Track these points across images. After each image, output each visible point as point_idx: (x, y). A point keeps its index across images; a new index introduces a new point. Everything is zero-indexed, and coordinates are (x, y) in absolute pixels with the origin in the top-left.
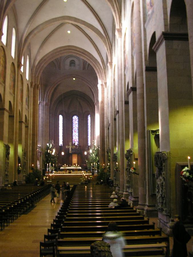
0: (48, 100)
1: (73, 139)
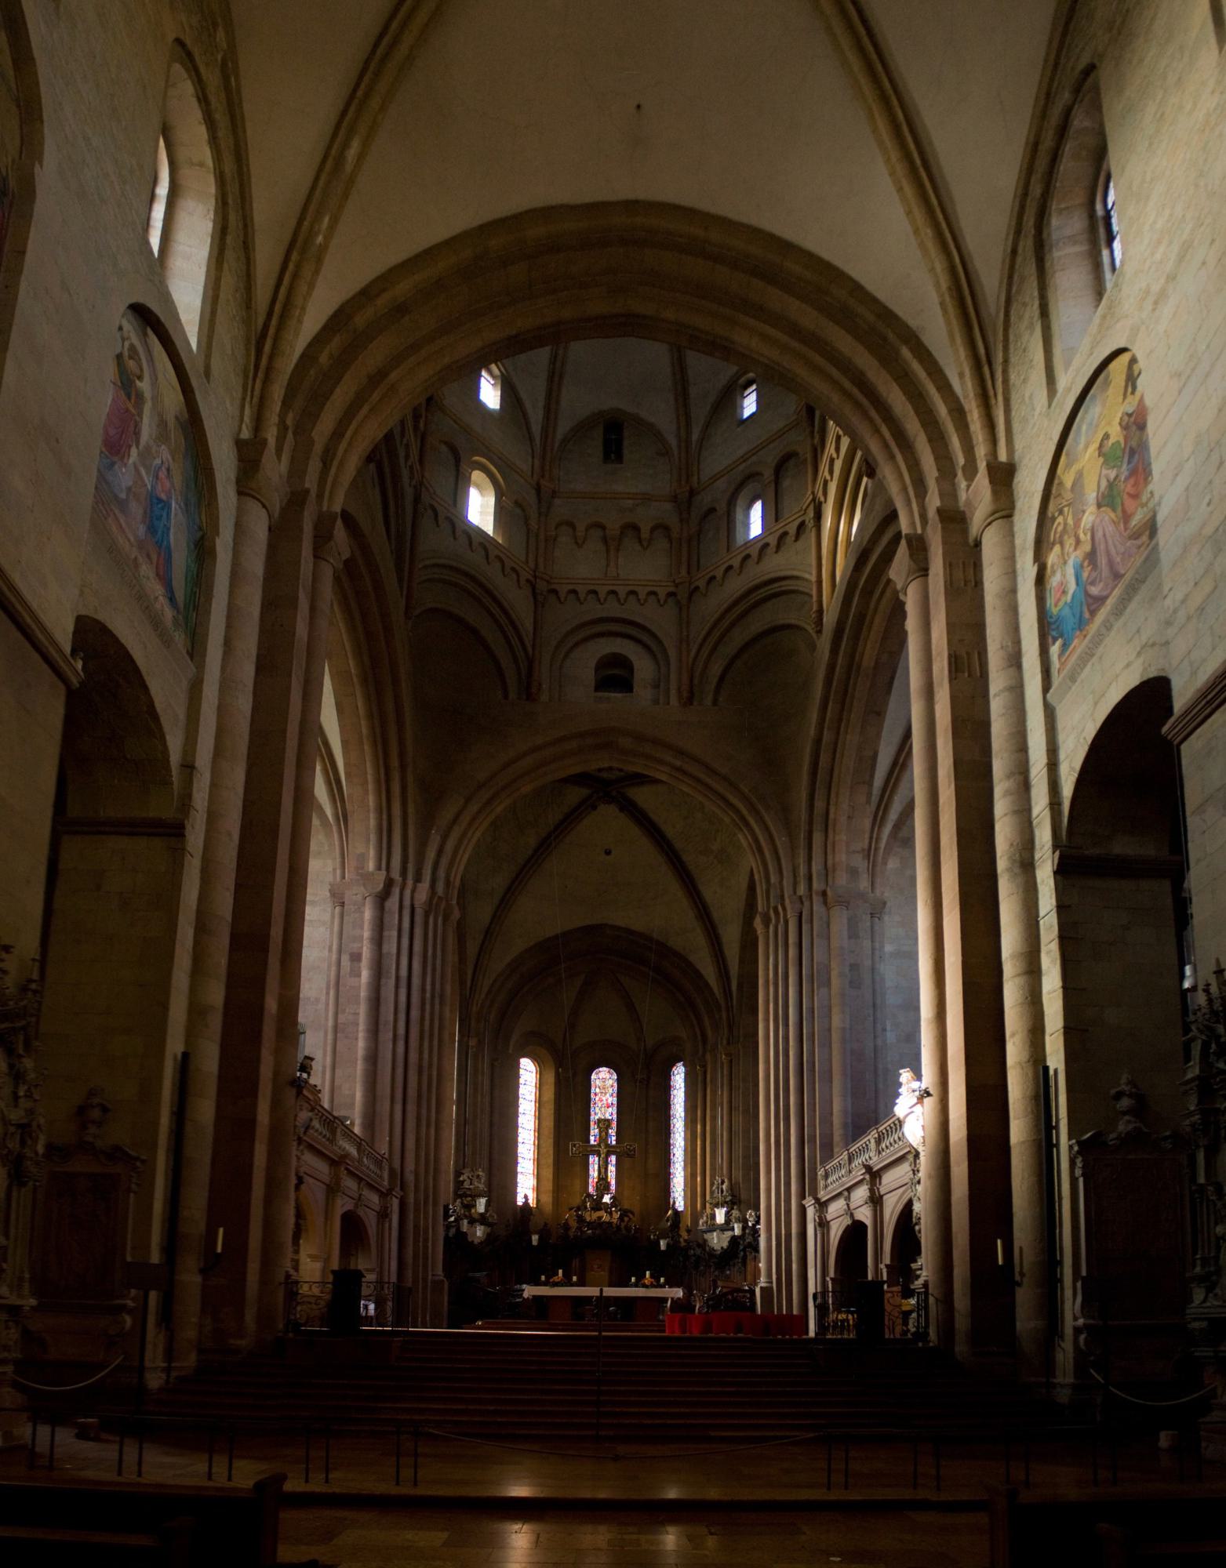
0: (448, 883)
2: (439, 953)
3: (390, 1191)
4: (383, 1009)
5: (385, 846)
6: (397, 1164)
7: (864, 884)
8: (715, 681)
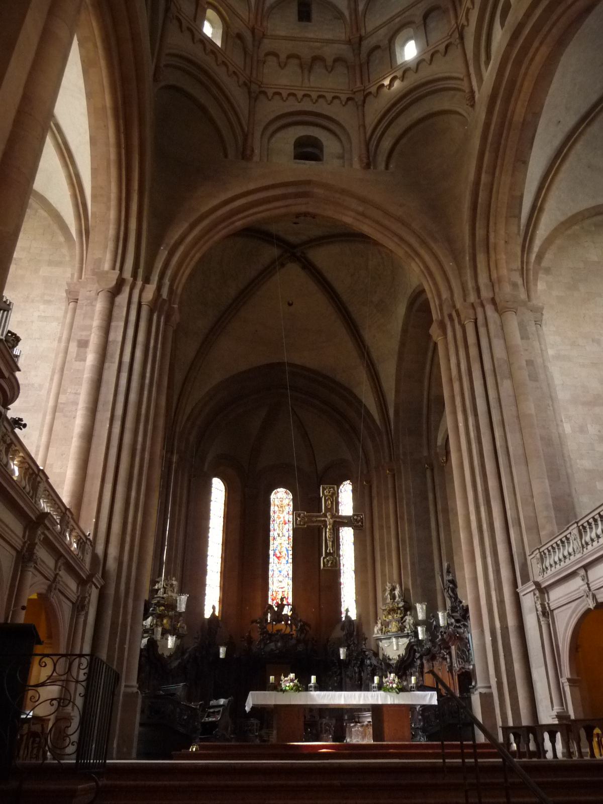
1: (270, 593)
3: (91, 577)
4: (103, 389)
5: (120, 251)
6: (100, 549)
7: (523, 296)
8: (386, 155)
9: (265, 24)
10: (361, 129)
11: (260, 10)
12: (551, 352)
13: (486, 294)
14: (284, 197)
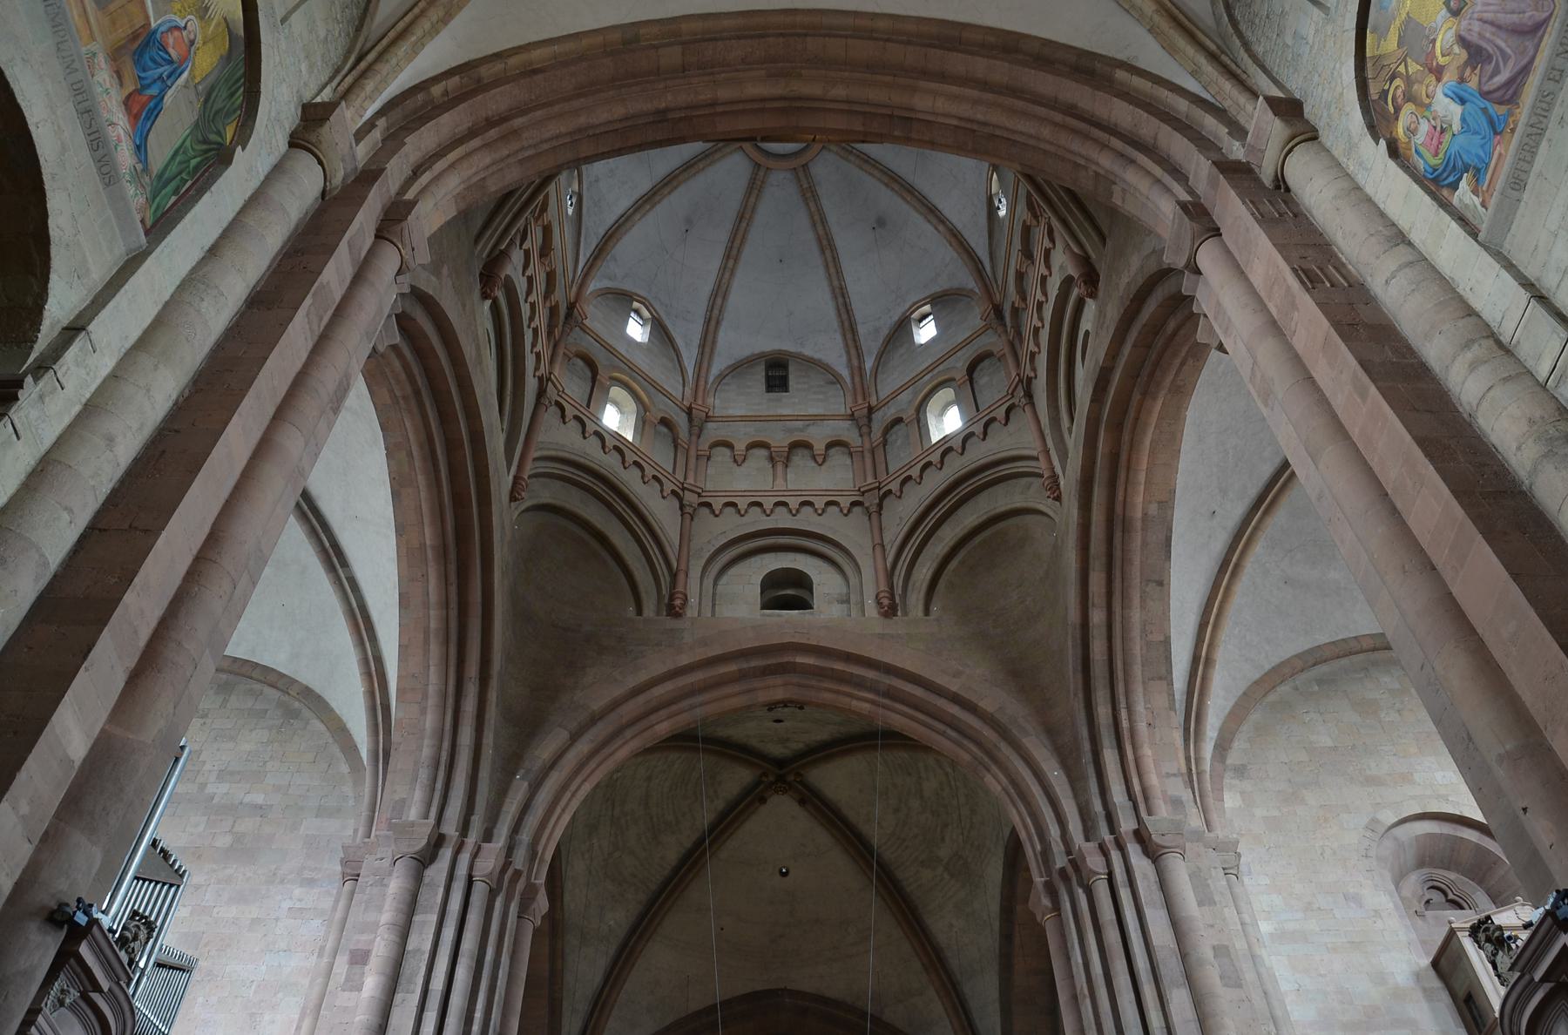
2: (505, 959)
7: (1195, 821)
9: (710, 400)
10: (878, 549)
11: (702, 383)
12: (1265, 927)
13: (1127, 825)
14: (742, 676)
